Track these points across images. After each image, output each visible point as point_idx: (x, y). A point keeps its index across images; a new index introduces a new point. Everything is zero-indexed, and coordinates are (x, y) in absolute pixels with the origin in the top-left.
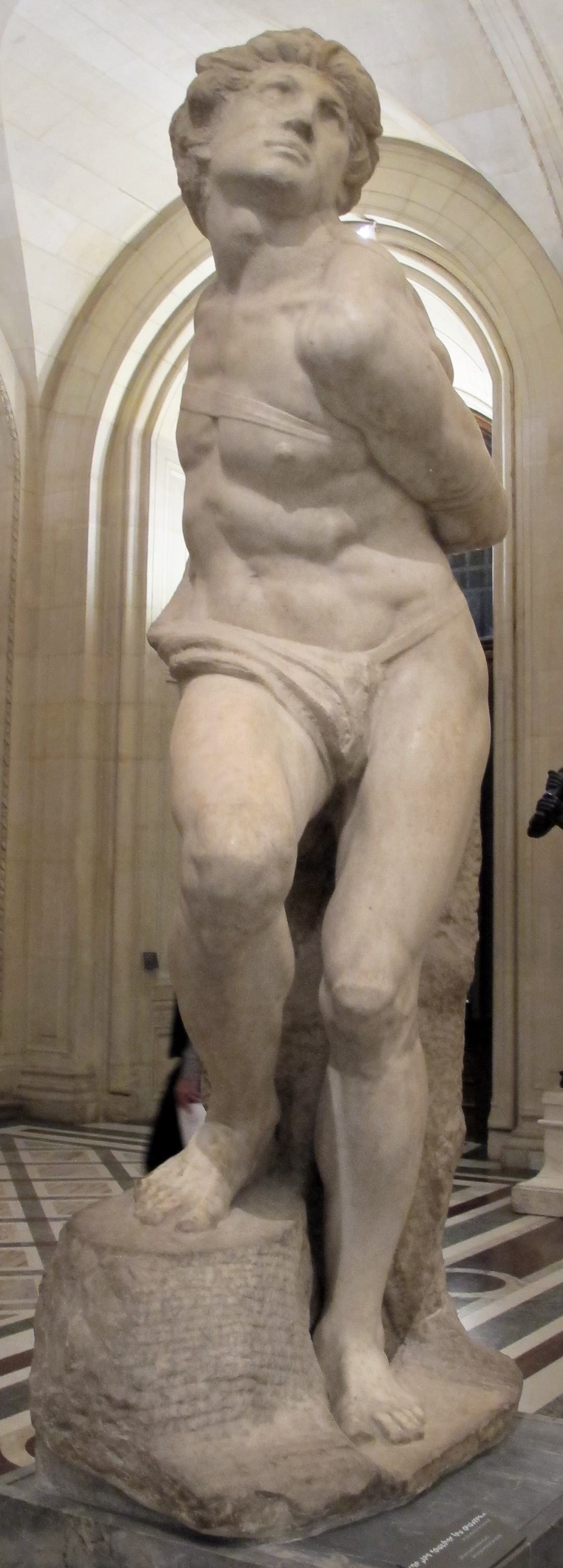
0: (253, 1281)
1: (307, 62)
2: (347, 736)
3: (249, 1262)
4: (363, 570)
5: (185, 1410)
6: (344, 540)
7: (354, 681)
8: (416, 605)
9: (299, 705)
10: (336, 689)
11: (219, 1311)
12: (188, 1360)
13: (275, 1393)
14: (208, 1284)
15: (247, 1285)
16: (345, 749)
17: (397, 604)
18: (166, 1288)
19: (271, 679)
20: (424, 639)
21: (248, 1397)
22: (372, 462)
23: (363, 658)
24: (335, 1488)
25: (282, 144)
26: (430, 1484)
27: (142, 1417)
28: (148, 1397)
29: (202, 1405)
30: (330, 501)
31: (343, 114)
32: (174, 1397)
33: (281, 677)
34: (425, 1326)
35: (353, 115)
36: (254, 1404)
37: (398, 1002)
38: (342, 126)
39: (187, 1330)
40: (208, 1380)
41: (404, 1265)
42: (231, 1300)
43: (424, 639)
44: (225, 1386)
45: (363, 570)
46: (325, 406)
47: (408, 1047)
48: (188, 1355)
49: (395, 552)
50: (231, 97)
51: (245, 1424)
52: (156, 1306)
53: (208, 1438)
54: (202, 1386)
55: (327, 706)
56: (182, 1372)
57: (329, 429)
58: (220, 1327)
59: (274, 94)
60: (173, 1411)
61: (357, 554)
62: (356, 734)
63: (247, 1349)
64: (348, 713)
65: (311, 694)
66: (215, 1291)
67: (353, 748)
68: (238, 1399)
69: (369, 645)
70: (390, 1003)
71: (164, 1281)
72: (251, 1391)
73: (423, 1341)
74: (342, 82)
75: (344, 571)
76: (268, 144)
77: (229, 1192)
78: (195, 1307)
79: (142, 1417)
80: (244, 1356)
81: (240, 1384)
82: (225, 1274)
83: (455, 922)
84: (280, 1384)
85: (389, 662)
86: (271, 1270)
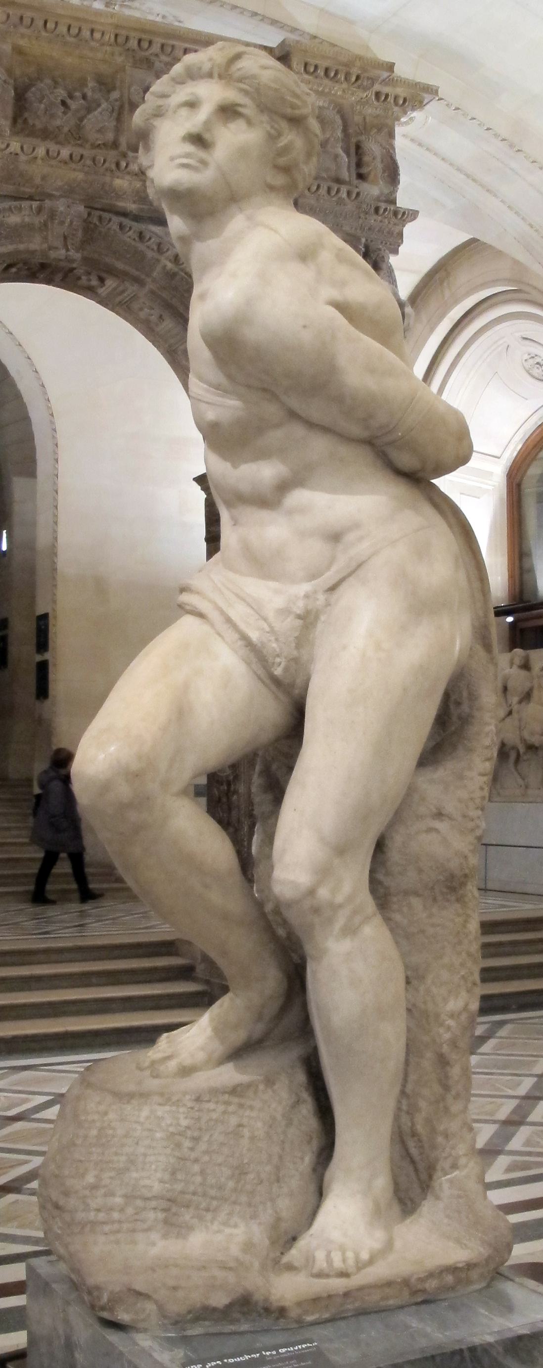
0: (184, 1123)
1: (210, 75)
2: (278, 660)
3: (185, 1105)
4: (302, 510)
5: (101, 1216)
6: (283, 487)
7: (284, 612)
8: (350, 537)
9: (237, 636)
10: (265, 619)
12: (111, 1178)
13: (201, 1218)
14: (142, 1119)
15: (179, 1125)
16: (278, 671)
17: (335, 537)
18: (106, 1118)
19: (213, 615)
20: (359, 566)
21: (161, 1216)
22: (293, 415)
23: (305, 587)
24: (197, 1298)
25: (180, 157)
26: (326, 1315)
27: (67, 1217)
28: (72, 1202)
29: (116, 1215)
30: (262, 455)
31: (249, 110)
32: (93, 1204)
33: (222, 613)
34: (441, 1185)
35: (263, 108)
36: (166, 1222)
37: (323, 893)
38: (249, 122)
39: (116, 1154)
40: (126, 1196)
41: (420, 1128)
42: (158, 1135)
43: (359, 566)
44: (139, 1203)
45: (302, 510)
46: (229, 377)
47: (350, 931)
48: (113, 1174)
49: (333, 491)
50: (157, 122)
51: (154, 1236)
52: (94, 1132)
53: (117, 1242)
54: (118, 1200)
55: (254, 636)
56: (105, 1186)
57: (240, 397)
58: (145, 1155)
59: (184, 112)
60: (92, 1215)
61: (299, 497)
62: (285, 658)
63: (167, 1177)
64: (277, 640)
65: (242, 626)
67: (286, 669)
68: (151, 1215)
69: (312, 577)
70: (311, 892)
71: (106, 1113)
72: (164, 1210)
73: (438, 1198)
74: (244, 83)
75: (290, 512)
76: (172, 159)
77: (219, 1049)
78: (126, 1136)
79: (67, 1217)
80: (161, 1181)
81: (154, 1203)
82: (159, 1113)
83: (450, 818)
84: (207, 1210)
85: (332, 589)
86: (214, 1116)
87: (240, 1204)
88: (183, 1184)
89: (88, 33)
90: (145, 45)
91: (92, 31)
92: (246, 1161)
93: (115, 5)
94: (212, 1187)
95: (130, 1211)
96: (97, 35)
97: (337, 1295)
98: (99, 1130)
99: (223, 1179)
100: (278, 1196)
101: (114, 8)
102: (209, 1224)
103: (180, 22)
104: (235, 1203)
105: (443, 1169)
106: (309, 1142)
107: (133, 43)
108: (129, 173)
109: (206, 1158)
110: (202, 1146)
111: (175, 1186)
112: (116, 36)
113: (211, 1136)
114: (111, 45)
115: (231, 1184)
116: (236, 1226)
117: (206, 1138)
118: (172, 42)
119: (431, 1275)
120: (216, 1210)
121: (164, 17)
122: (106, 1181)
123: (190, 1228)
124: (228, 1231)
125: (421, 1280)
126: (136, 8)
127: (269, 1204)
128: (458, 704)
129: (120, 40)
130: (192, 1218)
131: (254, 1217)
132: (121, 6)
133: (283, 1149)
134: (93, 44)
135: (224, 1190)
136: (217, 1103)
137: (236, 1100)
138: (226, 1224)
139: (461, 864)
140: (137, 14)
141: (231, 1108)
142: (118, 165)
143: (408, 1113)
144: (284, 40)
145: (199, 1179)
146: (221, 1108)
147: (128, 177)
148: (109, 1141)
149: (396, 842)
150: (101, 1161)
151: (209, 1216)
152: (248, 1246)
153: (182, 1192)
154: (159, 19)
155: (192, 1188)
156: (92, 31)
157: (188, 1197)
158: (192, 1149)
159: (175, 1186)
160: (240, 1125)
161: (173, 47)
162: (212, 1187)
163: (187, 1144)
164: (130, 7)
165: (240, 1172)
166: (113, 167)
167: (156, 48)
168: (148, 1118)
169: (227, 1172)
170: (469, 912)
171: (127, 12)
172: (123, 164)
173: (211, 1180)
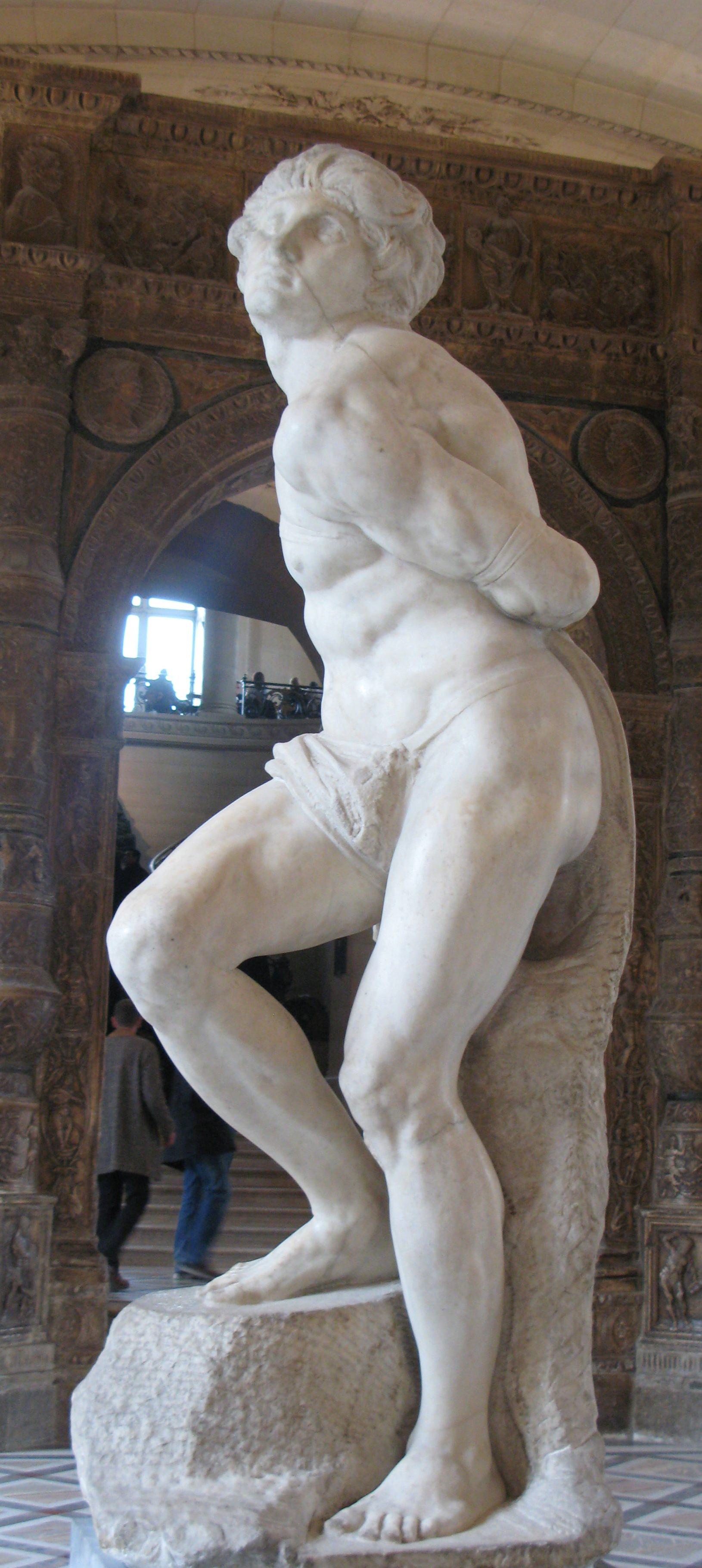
11: (182, 1368)
12: (141, 1405)
13: (237, 1459)
34: (547, 1461)
42: (197, 1360)
52: (128, 1353)
56: (133, 1413)
58: (180, 1381)
66: (186, 1347)
71: (142, 1335)
82: (201, 1336)
84: (247, 1450)
87: (289, 1450)
88: (220, 1417)
89: (413, 165)
90: (484, 175)
91: (418, 162)
92: (302, 1403)
93: (454, 128)
94: (255, 1425)
95: (155, 1443)
96: (424, 167)
97: (378, 1555)
98: (134, 1352)
99: (270, 1419)
100: (342, 1451)
101: (452, 133)
102: (247, 1467)
103: (536, 145)
104: (282, 1448)
105: (551, 1442)
106: (393, 1397)
107: (469, 175)
108: (463, 336)
109: (251, 1392)
110: (247, 1377)
111: (210, 1418)
112: (449, 166)
113: (261, 1367)
114: (442, 178)
115: (279, 1427)
116: (279, 1474)
117: (253, 1369)
118: (517, 170)
119: (501, 1550)
120: (257, 1453)
121: (515, 140)
122: (135, 1407)
123: (223, 1470)
124: (268, 1477)
125: (490, 1554)
126: (480, 132)
127: (326, 1457)
128: (590, 891)
129: (452, 169)
130: (227, 1457)
131: (306, 1467)
132: (461, 129)
133: (357, 1400)
134: (419, 178)
135: (271, 1431)
136: (270, 1330)
137: (295, 1331)
138: (269, 1470)
139: (574, 1071)
140: (482, 139)
141: (288, 1339)
142: (449, 325)
143: (512, 1371)
144: (661, 162)
145: (240, 1415)
146: (278, 1337)
147: (462, 340)
148: (143, 1363)
149: (500, 1041)
150: (132, 1385)
151: (247, 1459)
152: (290, 1497)
153: (219, 1426)
154: (509, 144)
155: (230, 1424)
156: (418, 162)
157: (223, 1433)
158: (236, 1379)
159: (210, 1418)
160: (296, 1361)
161: (520, 176)
162: (255, 1425)
163: (229, 1372)
164: (472, 131)
165: (294, 1416)
166: (444, 327)
167: (498, 180)
168: (187, 1340)
169: (277, 1411)
170: (587, 1132)
171: (469, 137)
172: (455, 323)
173: (255, 1417)
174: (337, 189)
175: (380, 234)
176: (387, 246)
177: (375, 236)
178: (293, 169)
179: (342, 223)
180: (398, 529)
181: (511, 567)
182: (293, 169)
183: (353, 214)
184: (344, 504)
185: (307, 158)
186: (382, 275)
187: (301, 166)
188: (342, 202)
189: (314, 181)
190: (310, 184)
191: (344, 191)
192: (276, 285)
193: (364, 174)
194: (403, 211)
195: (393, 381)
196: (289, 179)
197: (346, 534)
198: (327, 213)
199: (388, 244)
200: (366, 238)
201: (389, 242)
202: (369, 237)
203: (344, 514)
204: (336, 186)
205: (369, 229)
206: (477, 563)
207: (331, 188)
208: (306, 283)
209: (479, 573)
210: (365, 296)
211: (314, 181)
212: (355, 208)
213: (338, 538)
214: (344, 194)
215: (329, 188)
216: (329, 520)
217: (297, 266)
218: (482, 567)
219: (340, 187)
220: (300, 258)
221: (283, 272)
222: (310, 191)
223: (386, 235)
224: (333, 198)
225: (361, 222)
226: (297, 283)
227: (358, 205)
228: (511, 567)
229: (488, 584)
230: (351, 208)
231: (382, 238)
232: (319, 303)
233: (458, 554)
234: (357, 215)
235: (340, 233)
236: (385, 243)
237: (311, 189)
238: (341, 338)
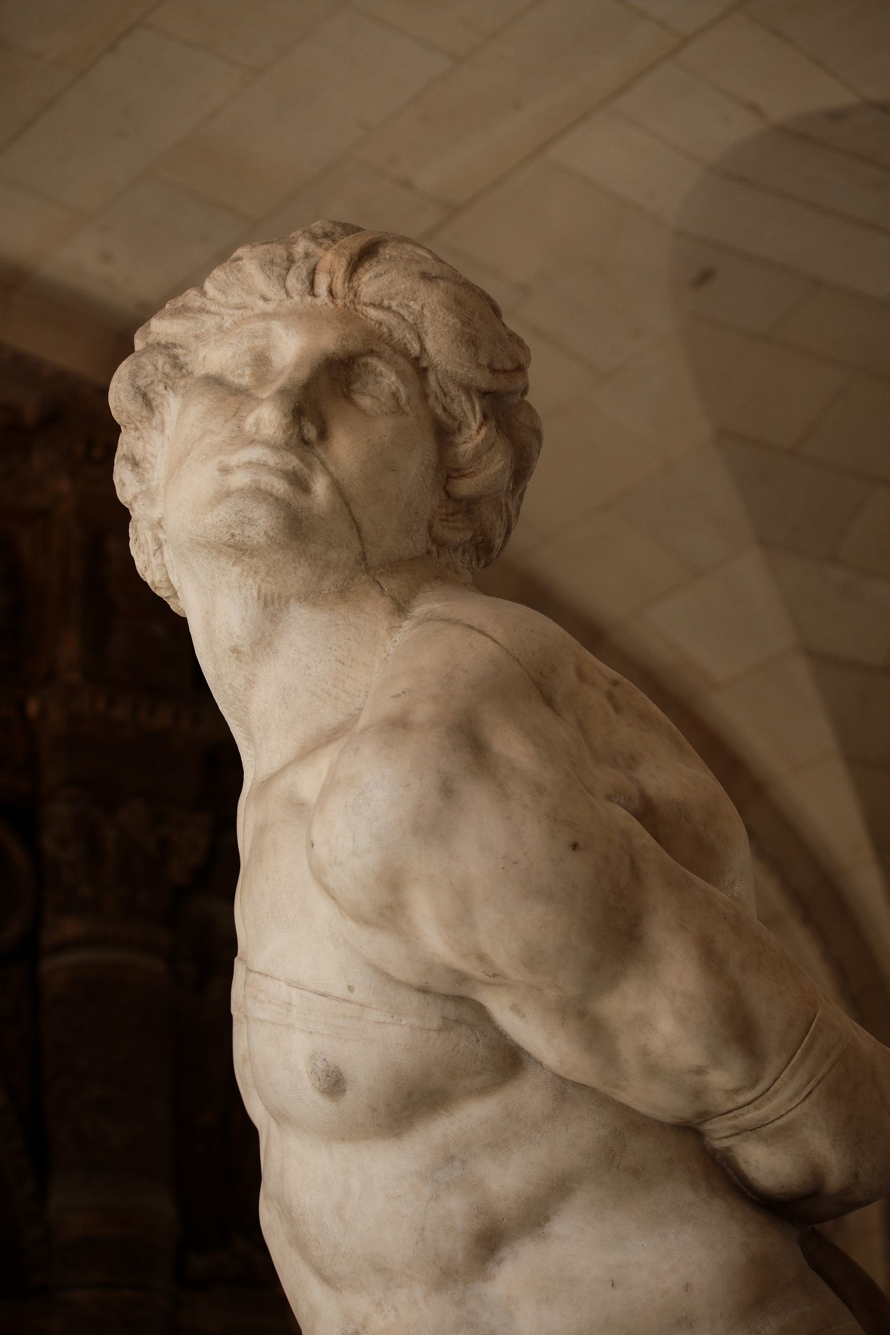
174: (389, 308)
175: (467, 406)
176: (478, 432)
177: (456, 409)
178: (291, 260)
179: (400, 375)
180: (582, 1014)
181: (804, 1100)
182: (291, 260)
183: (417, 359)
184: (482, 958)
185: (314, 237)
186: (465, 487)
187: (307, 256)
188: (397, 335)
189: (339, 287)
190: (331, 292)
191: (403, 312)
192: (280, 486)
193: (442, 284)
194: (509, 365)
195: (549, 701)
196: (282, 279)
197: (458, 1021)
198: (371, 353)
199: (480, 428)
200: (439, 411)
201: (482, 425)
202: (445, 409)
203: (462, 978)
204: (386, 303)
205: (445, 395)
206: (737, 1091)
207: (378, 306)
208: (337, 487)
209: (730, 1111)
210: (430, 527)
211: (339, 287)
212: (423, 349)
213: (440, 1030)
214: (404, 319)
215: (373, 305)
216: (424, 991)
217: (320, 451)
218: (742, 1099)
219: (394, 304)
220: (323, 434)
221: (293, 462)
222: (331, 305)
223: (477, 408)
224: (381, 324)
225: (432, 377)
226: (320, 486)
227: (430, 345)
228: (804, 1100)
229: (738, 1134)
230: (415, 348)
231: (470, 415)
232: (359, 531)
233: (700, 1071)
234: (424, 364)
235: (395, 395)
236: (475, 426)
237: (333, 302)
238: (401, 608)
